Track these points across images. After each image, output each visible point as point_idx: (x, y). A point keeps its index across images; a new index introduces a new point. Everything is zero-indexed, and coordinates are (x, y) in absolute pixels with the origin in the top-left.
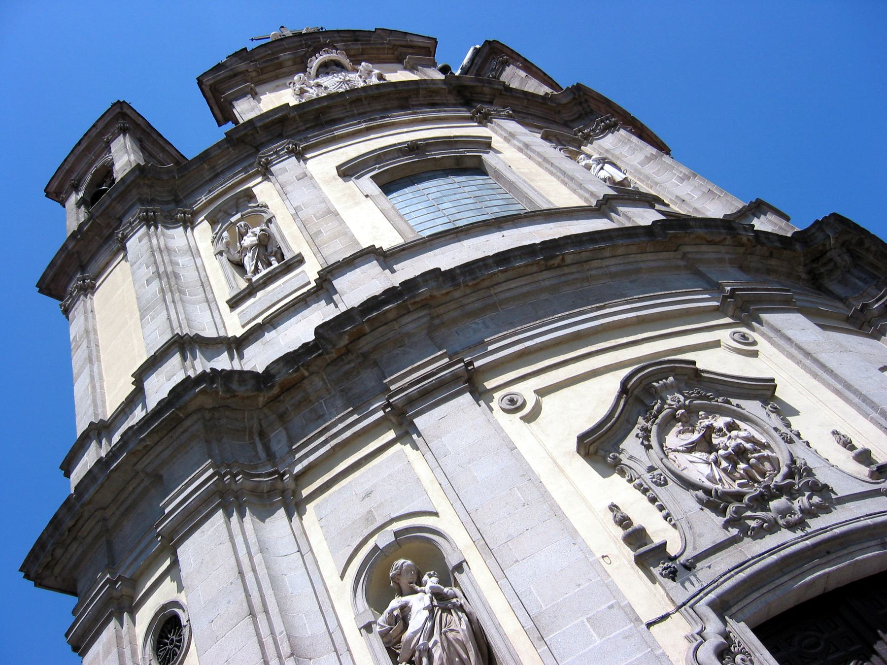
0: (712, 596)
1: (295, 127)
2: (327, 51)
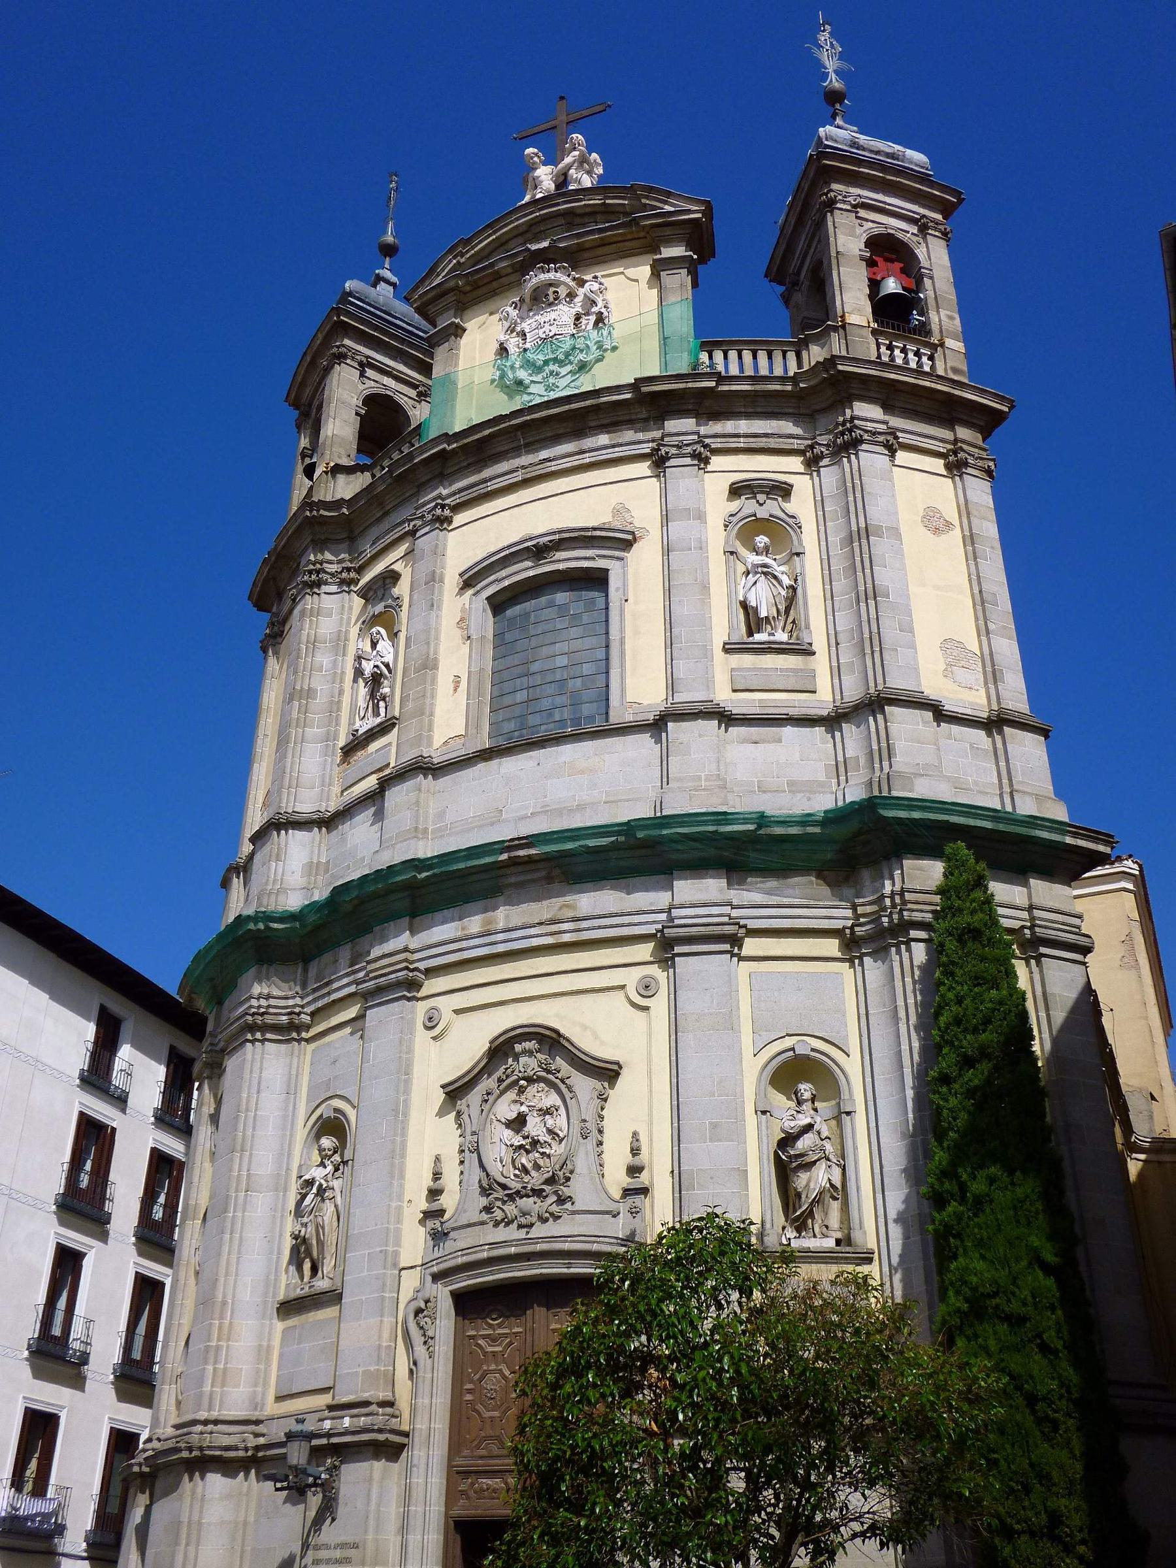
0: (435, 1269)
1: (457, 461)
2: (542, 267)
